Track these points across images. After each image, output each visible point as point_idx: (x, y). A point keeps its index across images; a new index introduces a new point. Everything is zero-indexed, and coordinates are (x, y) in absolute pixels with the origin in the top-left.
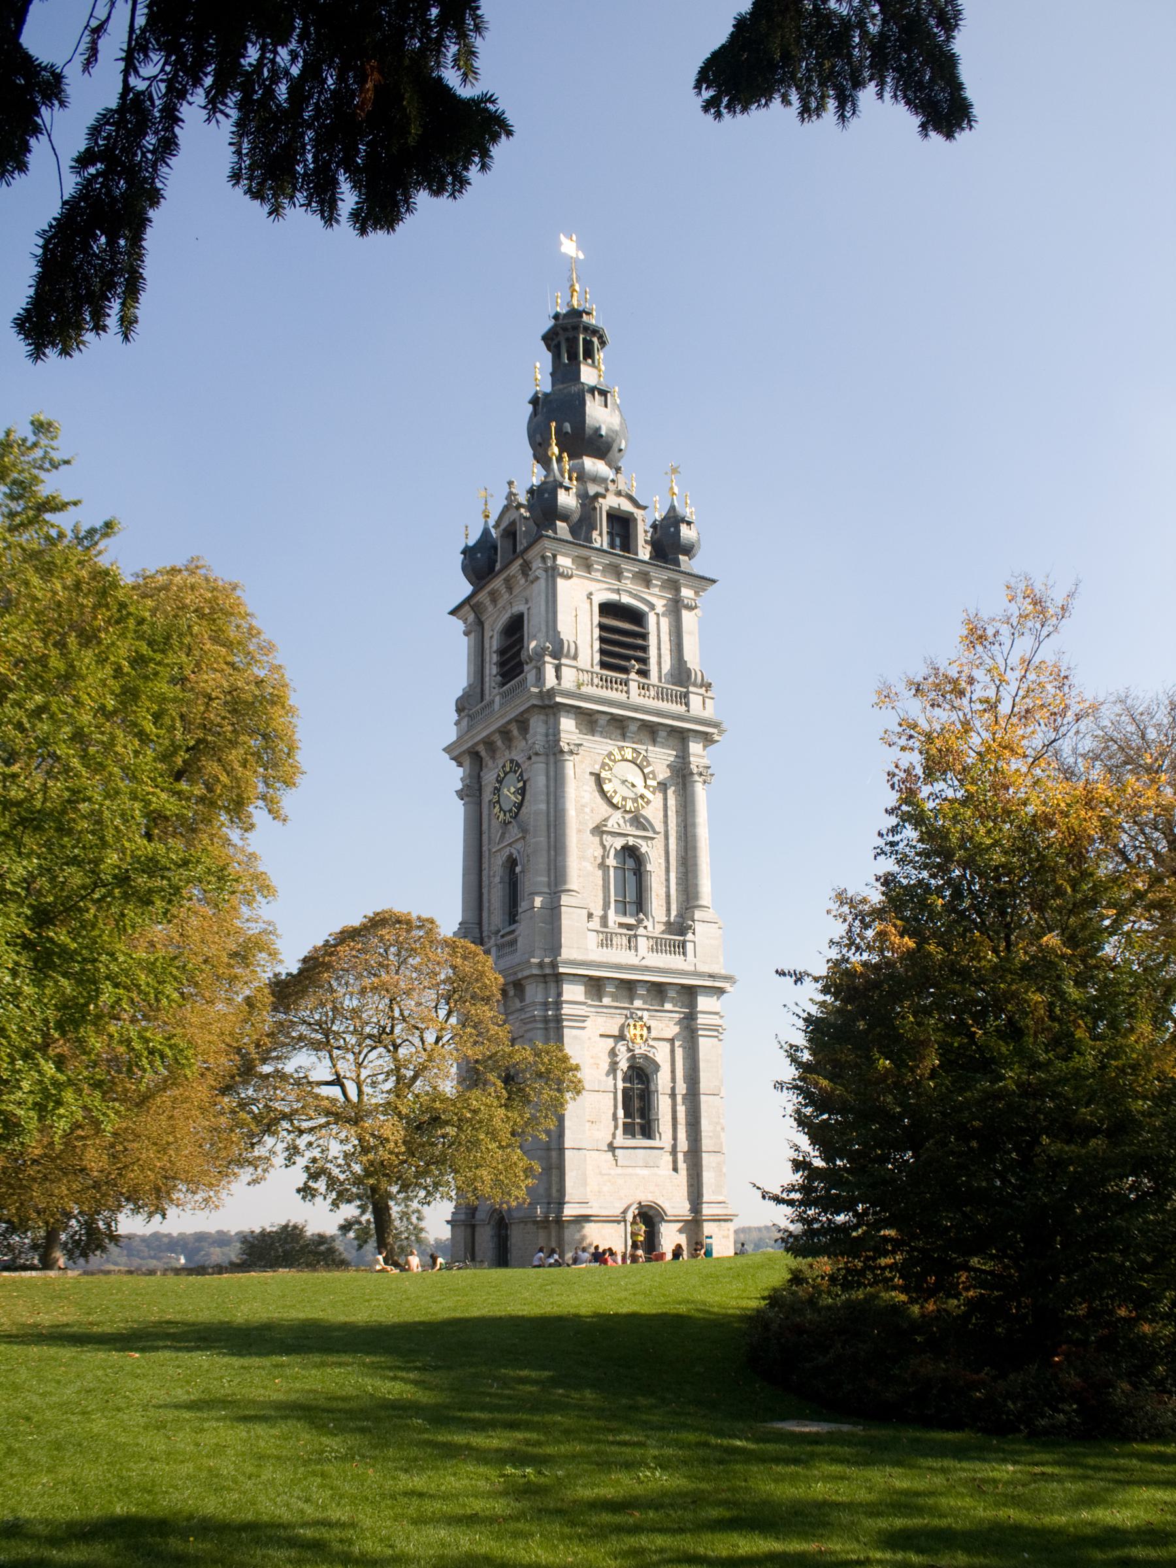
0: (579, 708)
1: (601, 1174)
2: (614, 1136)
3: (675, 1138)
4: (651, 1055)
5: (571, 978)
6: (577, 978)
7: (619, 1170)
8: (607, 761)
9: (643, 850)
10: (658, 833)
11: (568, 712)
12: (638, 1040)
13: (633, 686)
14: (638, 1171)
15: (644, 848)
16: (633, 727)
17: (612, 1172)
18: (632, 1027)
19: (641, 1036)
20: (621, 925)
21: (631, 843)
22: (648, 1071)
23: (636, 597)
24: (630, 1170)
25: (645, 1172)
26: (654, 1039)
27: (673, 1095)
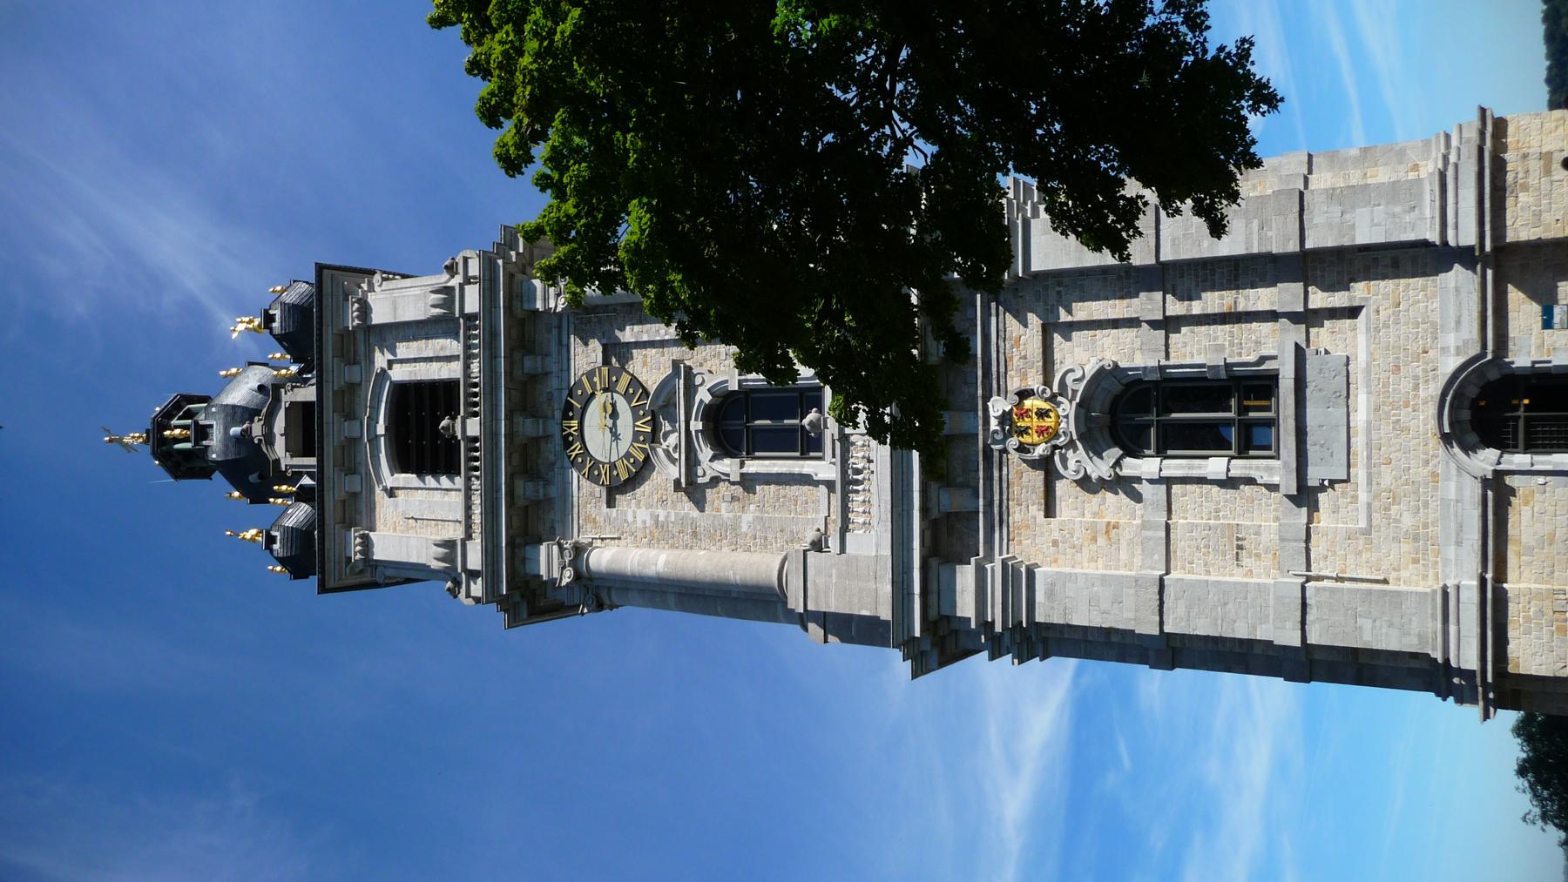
0: (511, 543)
1: (1367, 532)
2: (1273, 488)
3: (1272, 316)
4: (1081, 387)
5: (933, 599)
6: (933, 587)
7: (1359, 473)
8: (587, 469)
9: (708, 398)
10: (676, 364)
11: (524, 560)
12: (1049, 422)
13: (474, 427)
14: (1360, 418)
15: (704, 396)
16: (527, 427)
17: (1363, 497)
18: (1026, 439)
19: (1042, 414)
20: (834, 456)
21: (700, 426)
22: (1119, 388)
23: (375, 409)
24: (1359, 442)
25: (1361, 402)
26: (1047, 382)
27: (1169, 325)
